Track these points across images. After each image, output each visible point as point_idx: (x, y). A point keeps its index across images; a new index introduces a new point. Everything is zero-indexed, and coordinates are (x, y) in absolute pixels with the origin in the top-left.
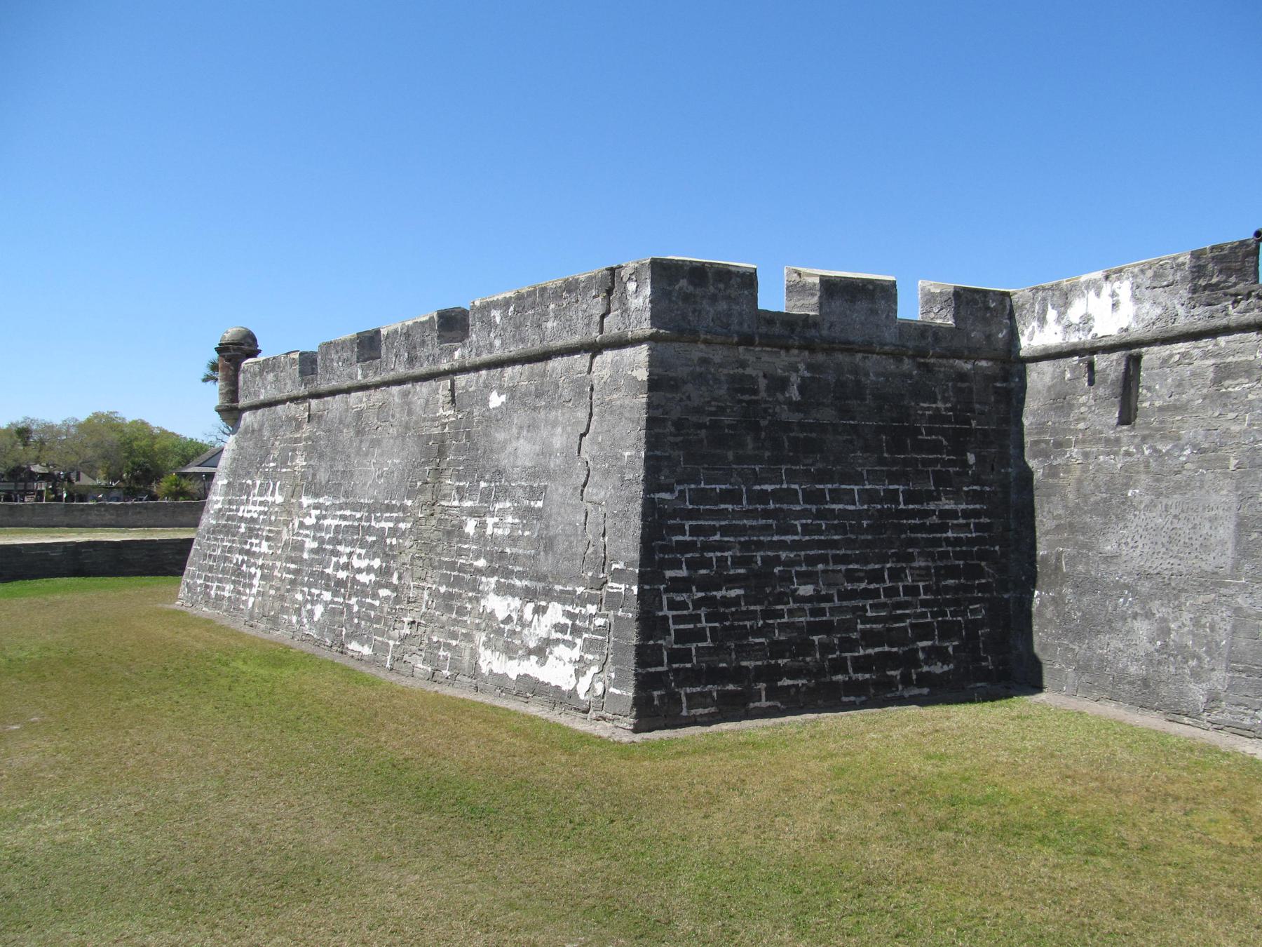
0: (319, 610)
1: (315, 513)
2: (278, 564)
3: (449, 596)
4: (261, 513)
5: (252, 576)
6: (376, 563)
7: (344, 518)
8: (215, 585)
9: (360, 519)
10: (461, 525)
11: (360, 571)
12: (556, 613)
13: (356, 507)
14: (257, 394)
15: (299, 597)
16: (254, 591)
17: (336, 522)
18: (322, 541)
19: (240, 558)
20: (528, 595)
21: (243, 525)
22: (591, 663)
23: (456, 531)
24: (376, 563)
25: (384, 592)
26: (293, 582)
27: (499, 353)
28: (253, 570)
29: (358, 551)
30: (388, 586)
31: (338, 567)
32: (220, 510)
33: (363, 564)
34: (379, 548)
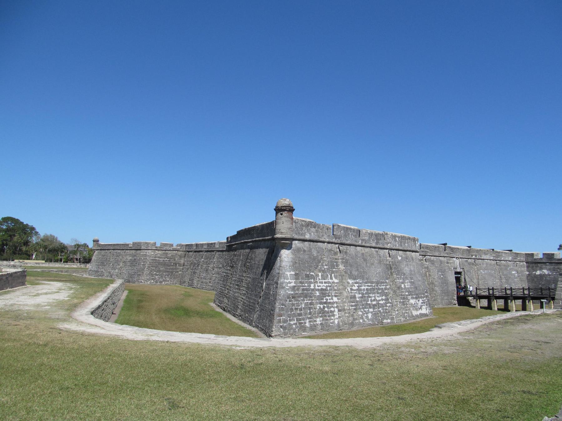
0: (370, 315)
1: (356, 285)
2: (346, 304)
3: (403, 302)
4: (327, 287)
6: (384, 297)
10: (401, 286)
11: (380, 300)
12: (421, 301)
13: (372, 283)
14: (304, 234)
15: (361, 313)
16: (337, 317)
18: (363, 294)
19: (322, 306)
20: (416, 298)
21: (317, 292)
23: (399, 288)
25: (388, 305)
26: (355, 309)
27: (397, 248)
28: (332, 309)
30: (389, 303)
32: (294, 287)
33: (380, 298)
34: (383, 294)
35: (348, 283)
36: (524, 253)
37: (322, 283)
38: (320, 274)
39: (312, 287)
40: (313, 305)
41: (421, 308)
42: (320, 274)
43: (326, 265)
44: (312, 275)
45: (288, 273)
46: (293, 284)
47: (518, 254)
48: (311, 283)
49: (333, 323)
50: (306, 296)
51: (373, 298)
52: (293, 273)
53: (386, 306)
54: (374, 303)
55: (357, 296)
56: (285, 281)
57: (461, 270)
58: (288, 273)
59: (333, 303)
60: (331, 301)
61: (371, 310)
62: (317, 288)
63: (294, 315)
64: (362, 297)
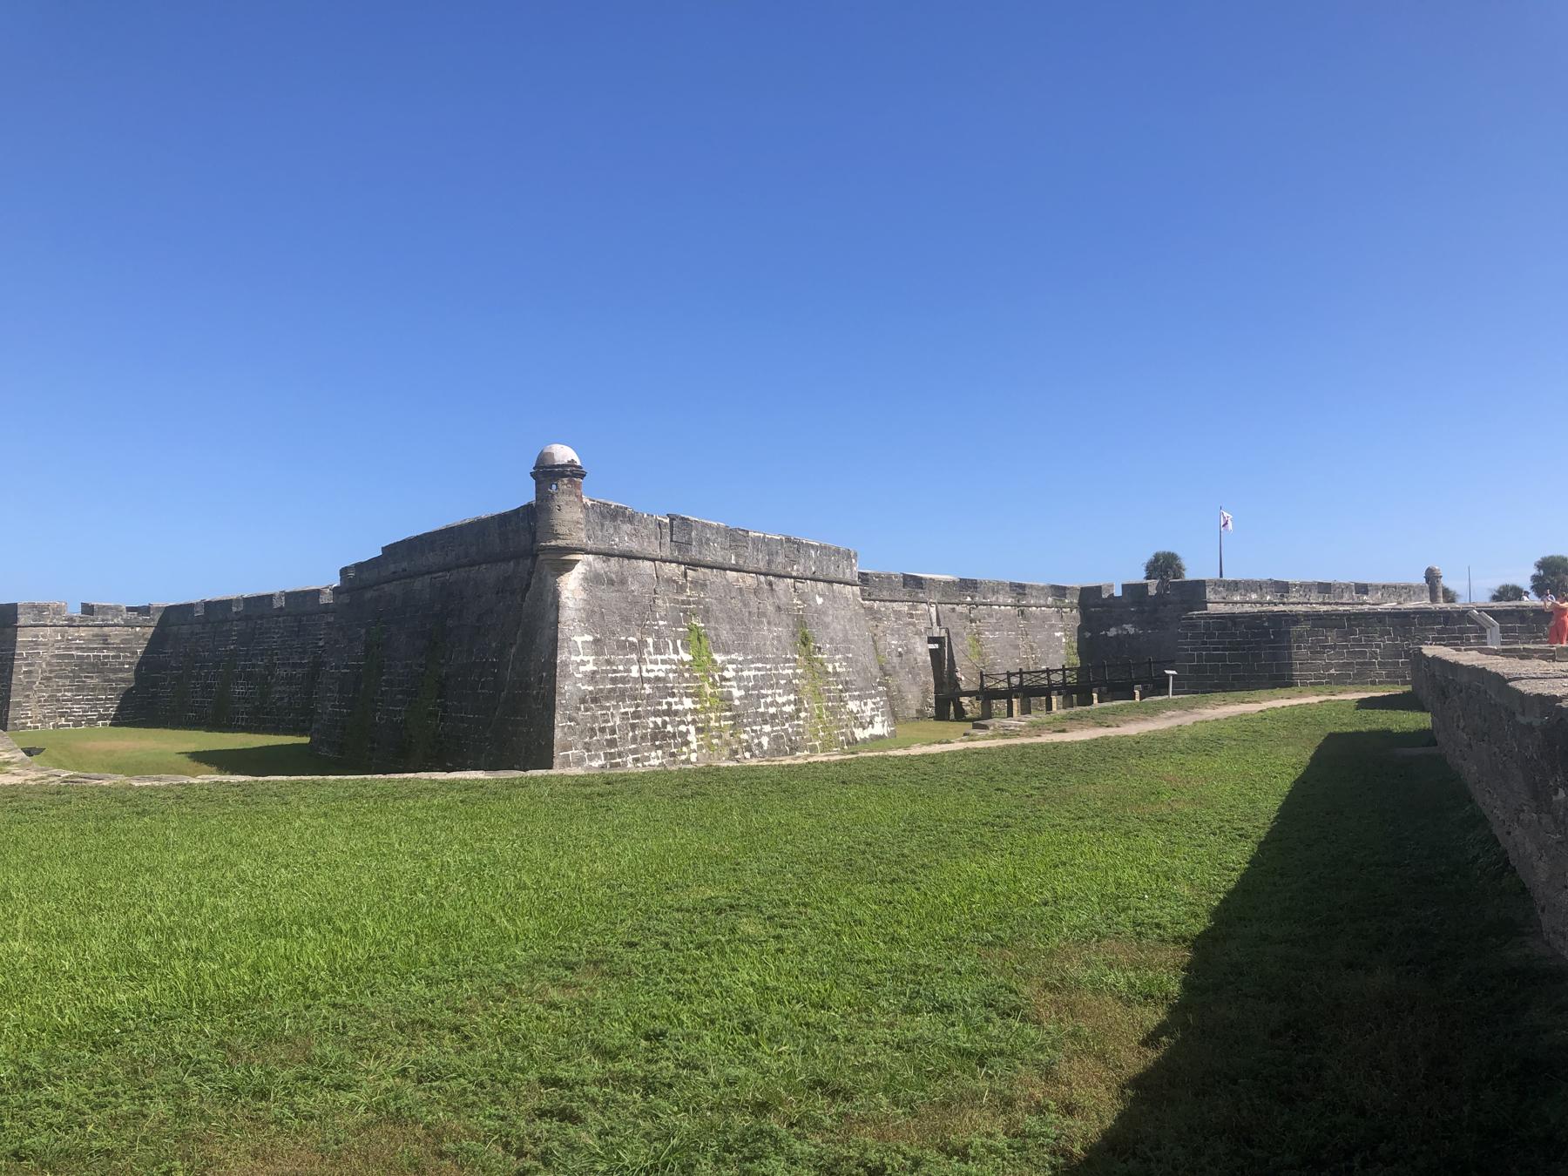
0: (765, 741)
1: (730, 667)
2: (712, 715)
5: (684, 735)
6: (792, 697)
7: (759, 669)
8: (631, 757)
13: (765, 661)
16: (694, 746)
17: (752, 673)
18: (747, 689)
20: (860, 698)
24: (792, 697)
28: (683, 728)
31: (767, 705)
32: (594, 672)
33: (784, 699)
35: (714, 662)
36: (1078, 585)
39: (635, 673)
40: (639, 717)
41: (871, 723)
42: (650, 641)
44: (632, 644)
45: (579, 639)
46: (590, 667)
47: (1065, 588)
48: (629, 662)
49: (688, 761)
50: (622, 696)
51: (769, 700)
52: (590, 638)
53: (798, 718)
54: (772, 710)
55: (737, 693)
56: (573, 658)
57: (943, 633)
58: (579, 639)
60: (680, 707)
61: (767, 728)
62: (645, 674)
63: (599, 745)
64: (745, 697)
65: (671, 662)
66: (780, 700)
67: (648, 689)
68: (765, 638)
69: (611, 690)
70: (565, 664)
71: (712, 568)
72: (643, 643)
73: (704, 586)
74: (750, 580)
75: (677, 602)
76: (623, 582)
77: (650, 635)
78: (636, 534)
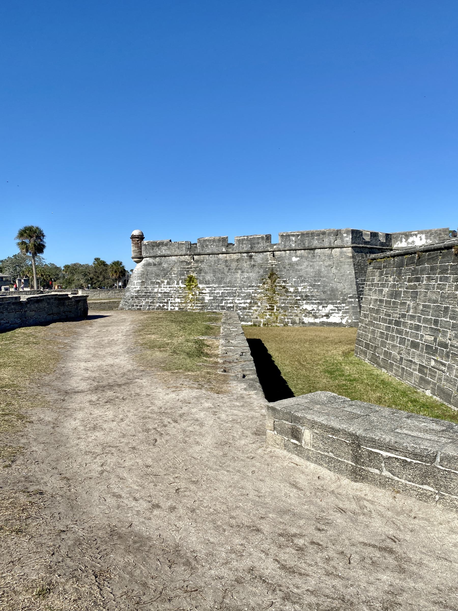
1: (207, 289)
6: (249, 301)
7: (227, 290)
9: (237, 290)
11: (240, 303)
22: (346, 316)
24: (249, 301)
29: (237, 298)
32: (139, 290)
35: (199, 288)
37: (166, 288)
38: (166, 281)
43: (174, 274)
44: (158, 282)
46: (138, 289)
48: (154, 287)
50: (148, 297)
51: (229, 301)
52: (141, 281)
54: (229, 305)
55: (207, 298)
56: (132, 286)
58: (135, 282)
59: (175, 303)
60: (173, 301)
62: (160, 291)
64: (213, 300)
65: (175, 287)
66: (236, 301)
67: (160, 295)
68: (236, 278)
69: (145, 295)
70: (129, 288)
71: (209, 254)
72: (163, 282)
73: (202, 262)
74: (235, 256)
75: (185, 268)
76: (160, 264)
77: (166, 279)
78: (169, 249)
